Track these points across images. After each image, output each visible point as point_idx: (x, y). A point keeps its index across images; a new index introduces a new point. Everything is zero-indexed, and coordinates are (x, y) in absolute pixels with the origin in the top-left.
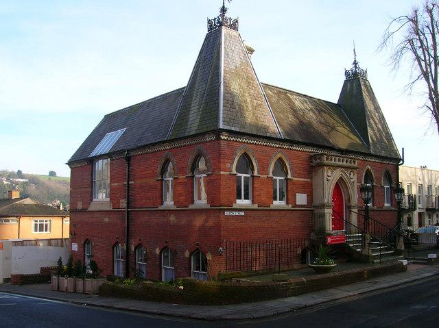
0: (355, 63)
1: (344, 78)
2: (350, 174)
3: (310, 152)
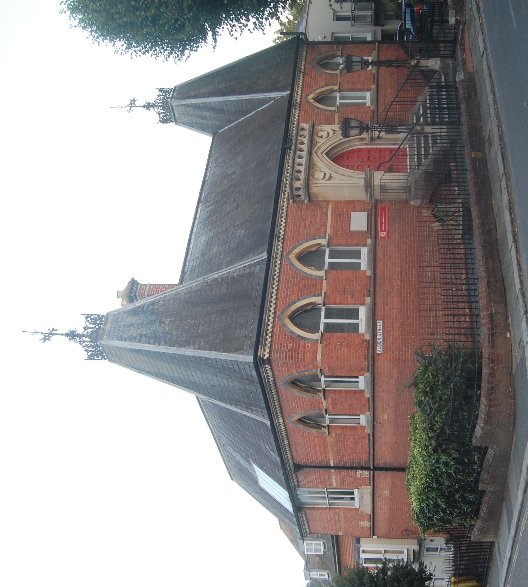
0: (148, 106)
1: (172, 125)
2: (322, 137)
3: (288, 203)
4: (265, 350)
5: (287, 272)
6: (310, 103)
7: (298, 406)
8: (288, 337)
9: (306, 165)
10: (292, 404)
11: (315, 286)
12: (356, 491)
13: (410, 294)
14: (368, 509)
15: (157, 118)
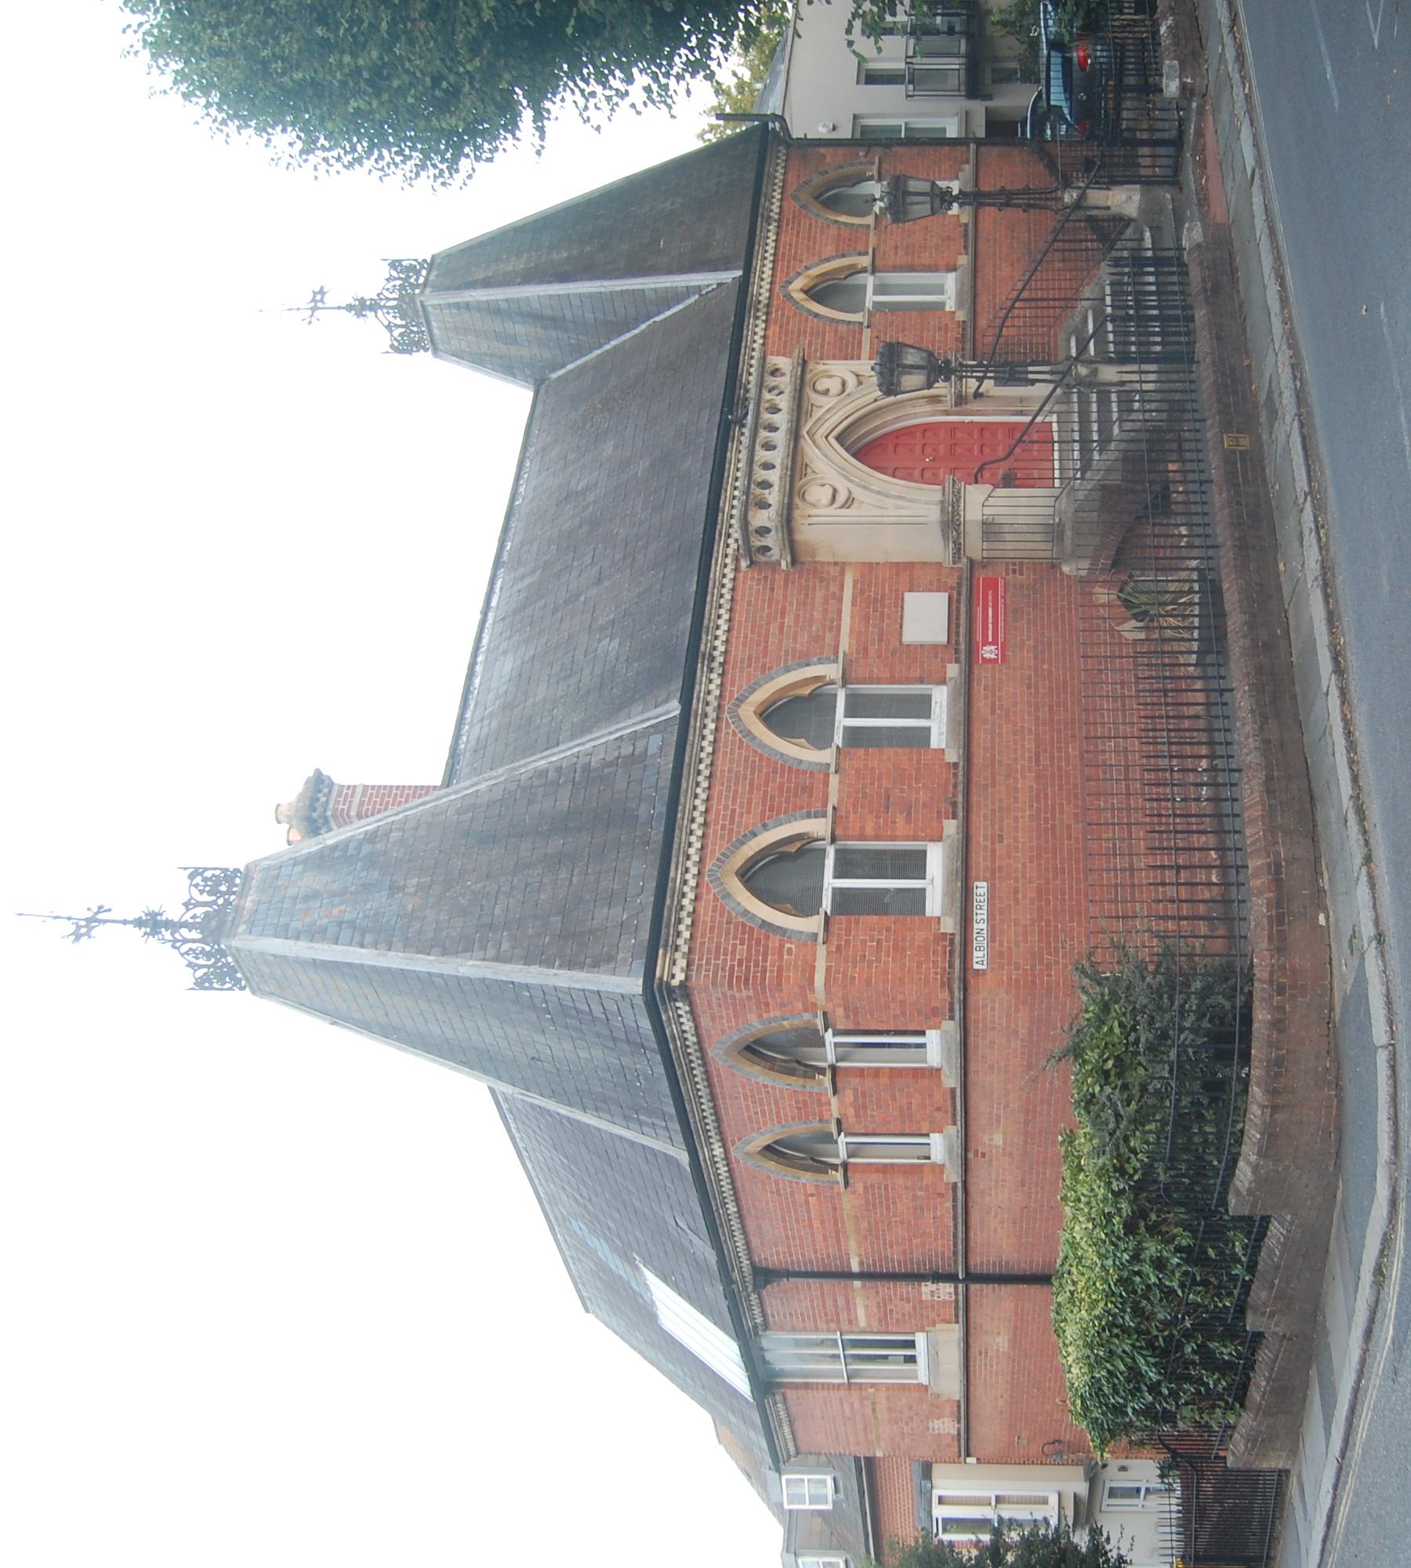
0: (361, 307)
2: (826, 392)
3: (736, 569)
4: (674, 962)
5: (732, 752)
6: (796, 303)
7: (763, 1112)
8: (736, 928)
9: (785, 467)
10: (748, 1107)
11: (809, 790)
12: (920, 1339)
13: (1061, 812)
14: (953, 1388)
15: (385, 339)
